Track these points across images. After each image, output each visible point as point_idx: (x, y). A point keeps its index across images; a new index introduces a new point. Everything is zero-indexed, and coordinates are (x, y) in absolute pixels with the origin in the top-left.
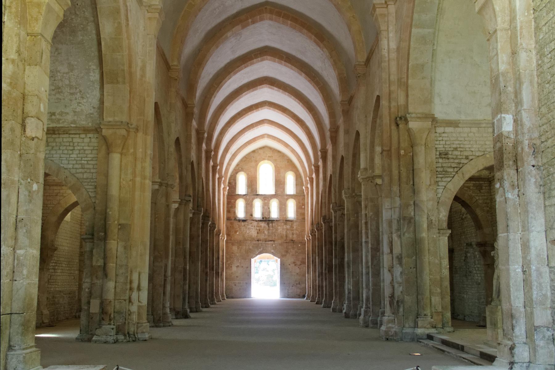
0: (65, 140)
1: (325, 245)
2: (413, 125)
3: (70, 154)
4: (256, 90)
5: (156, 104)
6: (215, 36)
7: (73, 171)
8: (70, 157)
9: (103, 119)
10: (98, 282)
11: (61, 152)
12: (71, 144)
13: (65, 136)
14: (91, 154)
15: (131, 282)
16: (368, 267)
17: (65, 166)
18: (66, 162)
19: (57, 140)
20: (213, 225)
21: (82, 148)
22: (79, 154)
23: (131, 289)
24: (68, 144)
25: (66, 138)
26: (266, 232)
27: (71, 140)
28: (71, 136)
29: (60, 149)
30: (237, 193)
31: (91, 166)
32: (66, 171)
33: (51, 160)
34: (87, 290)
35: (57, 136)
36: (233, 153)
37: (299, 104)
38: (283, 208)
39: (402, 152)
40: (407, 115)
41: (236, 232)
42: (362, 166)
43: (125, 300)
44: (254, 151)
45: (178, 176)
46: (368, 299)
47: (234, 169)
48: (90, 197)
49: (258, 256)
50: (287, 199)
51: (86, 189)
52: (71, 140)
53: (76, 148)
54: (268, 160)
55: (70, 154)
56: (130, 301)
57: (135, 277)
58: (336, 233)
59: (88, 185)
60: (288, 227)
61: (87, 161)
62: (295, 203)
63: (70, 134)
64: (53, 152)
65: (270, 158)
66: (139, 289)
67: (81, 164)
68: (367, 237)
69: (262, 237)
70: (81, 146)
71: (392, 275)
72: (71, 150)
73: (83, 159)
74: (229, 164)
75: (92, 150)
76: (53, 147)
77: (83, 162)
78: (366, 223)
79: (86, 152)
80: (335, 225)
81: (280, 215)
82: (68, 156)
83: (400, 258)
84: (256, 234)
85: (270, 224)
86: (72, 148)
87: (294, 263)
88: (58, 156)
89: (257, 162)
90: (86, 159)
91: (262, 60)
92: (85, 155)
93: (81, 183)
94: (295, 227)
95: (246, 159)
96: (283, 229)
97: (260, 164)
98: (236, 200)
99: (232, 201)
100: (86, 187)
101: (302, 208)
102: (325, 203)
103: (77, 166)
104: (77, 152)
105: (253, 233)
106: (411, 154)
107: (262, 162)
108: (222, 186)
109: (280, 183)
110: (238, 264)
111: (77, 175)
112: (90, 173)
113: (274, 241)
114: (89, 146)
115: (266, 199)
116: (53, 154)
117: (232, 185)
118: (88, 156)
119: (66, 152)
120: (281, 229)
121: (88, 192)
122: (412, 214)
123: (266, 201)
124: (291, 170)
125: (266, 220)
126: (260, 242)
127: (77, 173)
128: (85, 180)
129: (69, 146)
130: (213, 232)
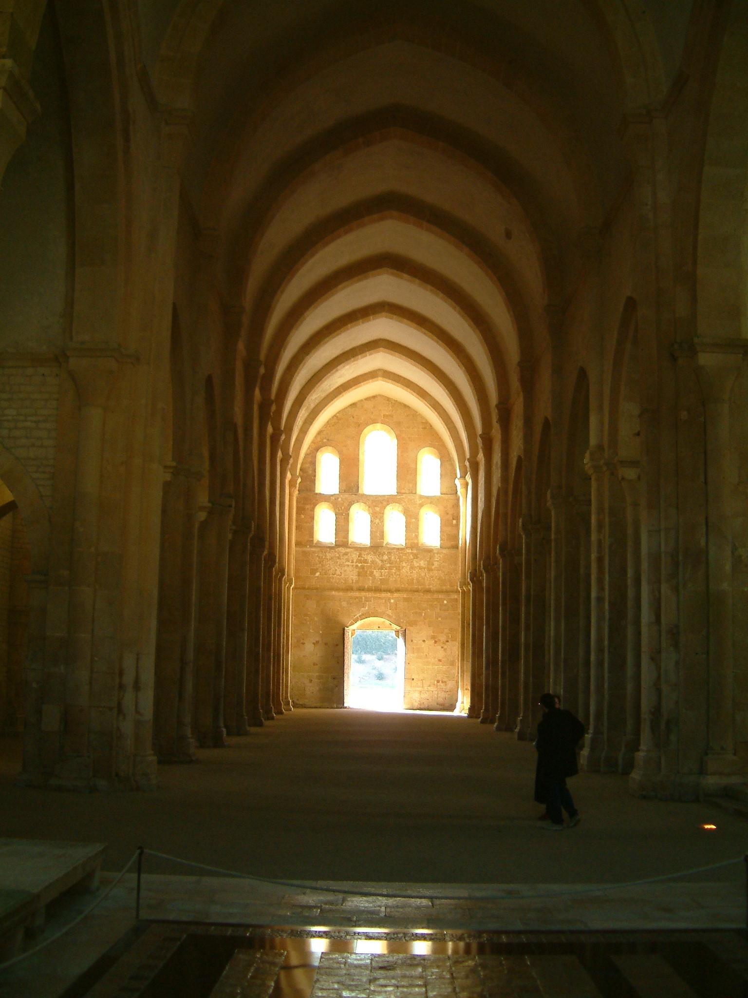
1: (504, 604)
2: (706, 359)
4: (366, 278)
5: (174, 304)
6: (290, 171)
9: (71, 338)
15: (121, 674)
16: (600, 650)
20: (271, 559)
23: (121, 687)
26: (376, 573)
30: (317, 491)
34: (35, 685)
36: (312, 406)
37: (454, 308)
39: (684, 415)
40: (696, 340)
41: (313, 572)
42: (593, 441)
43: (111, 709)
44: (353, 405)
45: (206, 454)
46: (599, 715)
47: (313, 442)
49: (359, 623)
50: (421, 505)
56: (120, 711)
57: (129, 663)
58: (528, 577)
60: (422, 563)
65: (386, 420)
66: (137, 687)
68: (601, 589)
69: (369, 583)
71: (659, 668)
73: (29, 418)
74: (304, 431)
77: (28, 424)
78: (600, 560)
80: (528, 561)
83: (674, 633)
84: (355, 578)
89: (360, 427)
90: (33, 418)
91: (382, 219)
94: (436, 564)
95: (337, 420)
96: (412, 568)
97: (365, 431)
98: (315, 505)
99: (307, 507)
101: (452, 525)
102: (505, 515)
105: (351, 575)
106: (702, 419)
107: (370, 427)
108: (289, 476)
109: (406, 472)
115: (376, 505)
120: (408, 571)
122: (703, 542)
123: (378, 509)
124: (431, 446)
125: (377, 546)
126: (363, 594)
130: (271, 572)
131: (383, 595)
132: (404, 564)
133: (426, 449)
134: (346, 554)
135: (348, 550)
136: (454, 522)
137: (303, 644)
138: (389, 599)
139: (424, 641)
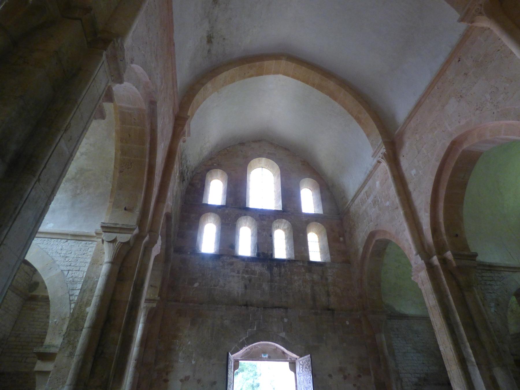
30: (203, 202)
38: (298, 242)
50: (307, 223)
54: (268, 157)
60: (316, 277)
62: (324, 231)
81: (295, 252)
85: (275, 269)
87: (341, 370)
94: (330, 279)
105: (235, 286)
110: (188, 373)
113: (286, 308)
117: (196, 188)
123: (265, 223)
126: (251, 309)
131: (275, 312)
132: (296, 278)
133: (307, 179)
134: (232, 264)
135: (234, 260)
136: (341, 239)
137: (166, 381)
138: (282, 318)
139: (330, 376)
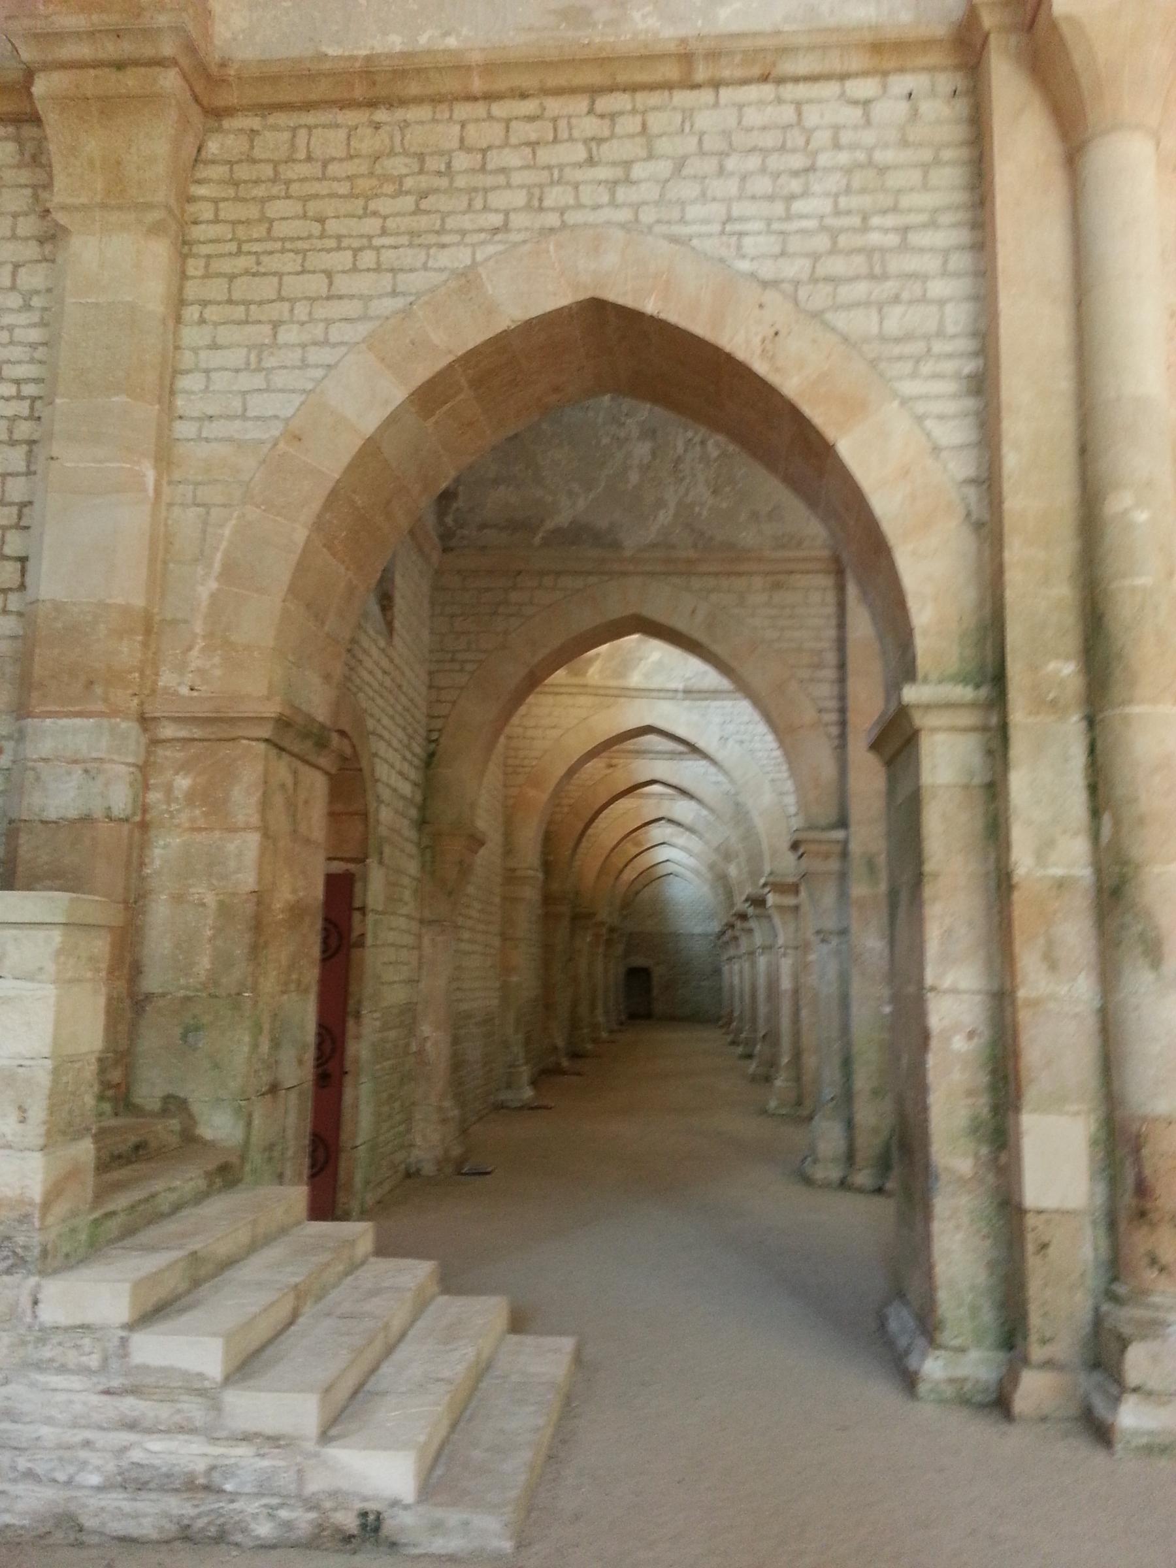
0: (753, 117)
3: (792, 197)
7: (819, 297)
8: (788, 217)
10: (1063, 990)
11: (731, 187)
12: (796, 138)
13: (753, 92)
14: (925, 187)
17: (767, 270)
18: (769, 244)
19: (704, 120)
21: (861, 156)
22: (848, 191)
24: (769, 140)
25: (761, 103)
27: (787, 113)
28: (790, 91)
29: (721, 171)
31: (930, 264)
32: (770, 296)
33: (674, 239)
35: (706, 95)
48: (936, 450)
51: (905, 401)
52: (787, 113)
53: (823, 160)
55: (792, 197)
59: (914, 375)
61: (905, 230)
63: (781, 81)
64: (689, 190)
67: (869, 252)
70: (853, 147)
72: (795, 174)
73: (876, 221)
75: (925, 167)
76: (680, 164)
77: (875, 238)
79: (895, 180)
82: (779, 208)
86: (798, 161)
88: (717, 210)
90: (890, 221)
92: (886, 201)
93: (873, 363)
100: (908, 387)
103: (836, 266)
104: (834, 182)
111: (840, 320)
112: (923, 299)
114: (904, 143)
116: (682, 203)
118: (905, 201)
119: (762, 185)
121: (920, 419)
127: (837, 308)
128: (897, 350)
129: (783, 148)
